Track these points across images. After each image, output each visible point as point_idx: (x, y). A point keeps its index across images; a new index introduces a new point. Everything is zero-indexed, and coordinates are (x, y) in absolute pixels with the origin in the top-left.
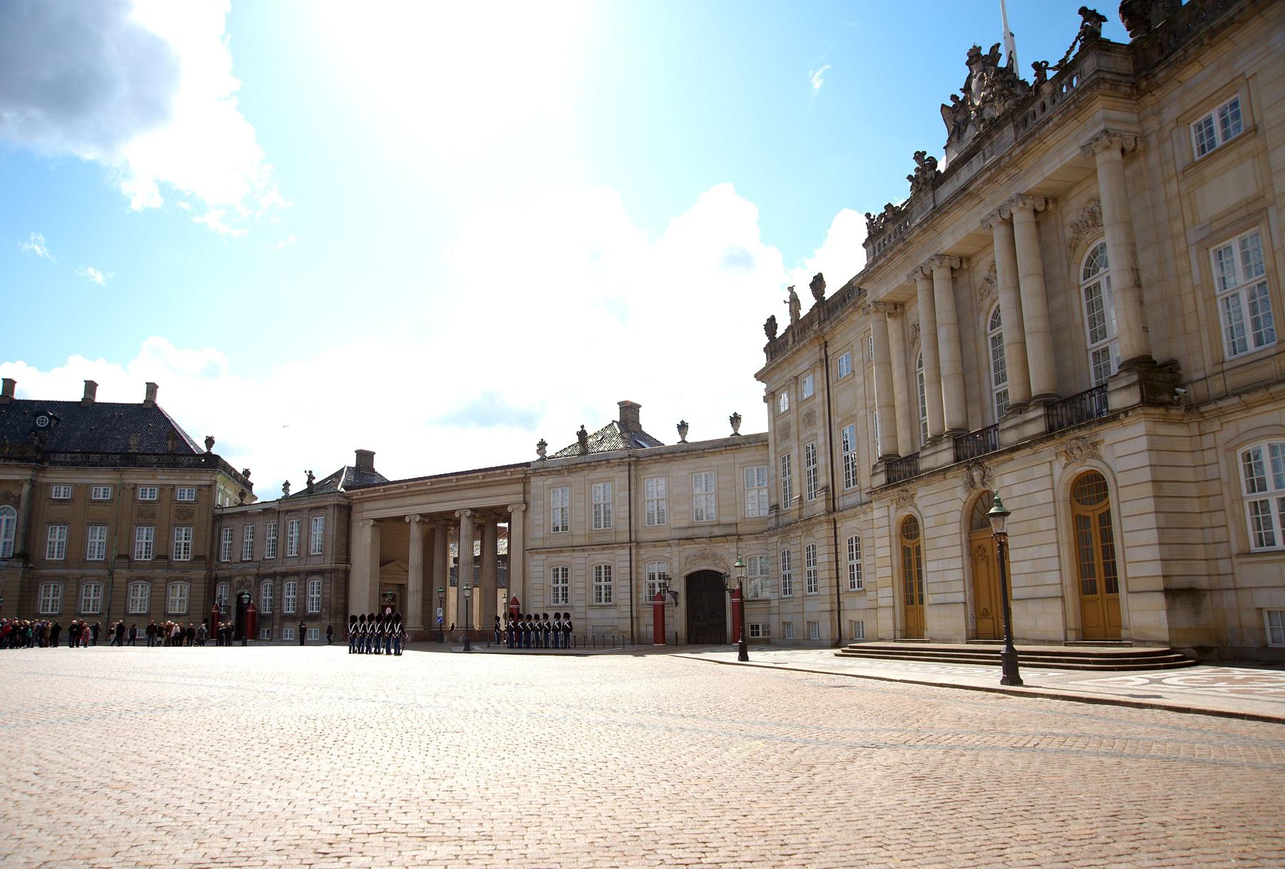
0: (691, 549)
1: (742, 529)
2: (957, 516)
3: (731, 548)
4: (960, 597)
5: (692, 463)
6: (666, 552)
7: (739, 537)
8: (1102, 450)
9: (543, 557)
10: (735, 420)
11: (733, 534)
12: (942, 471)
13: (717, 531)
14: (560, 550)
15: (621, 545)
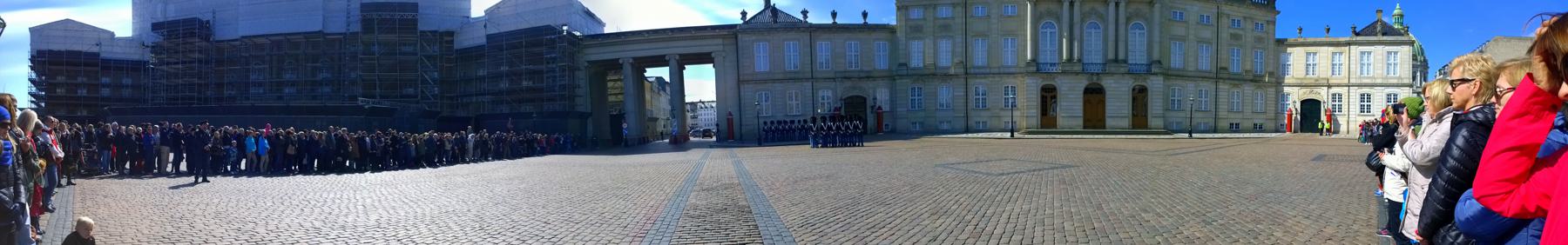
0: (848, 84)
1: (876, 74)
2: (1083, 89)
3: (871, 84)
4: (1081, 115)
5: (846, 35)
6: (832, 85)
7: (874, 78)
8: (1148, 81)
9: (751, 86)
10: (865, 15)
11: (869, 77)
12: (1077, 74)
13: (862, 75)
14: (765, 81)
15: (807, 79)
